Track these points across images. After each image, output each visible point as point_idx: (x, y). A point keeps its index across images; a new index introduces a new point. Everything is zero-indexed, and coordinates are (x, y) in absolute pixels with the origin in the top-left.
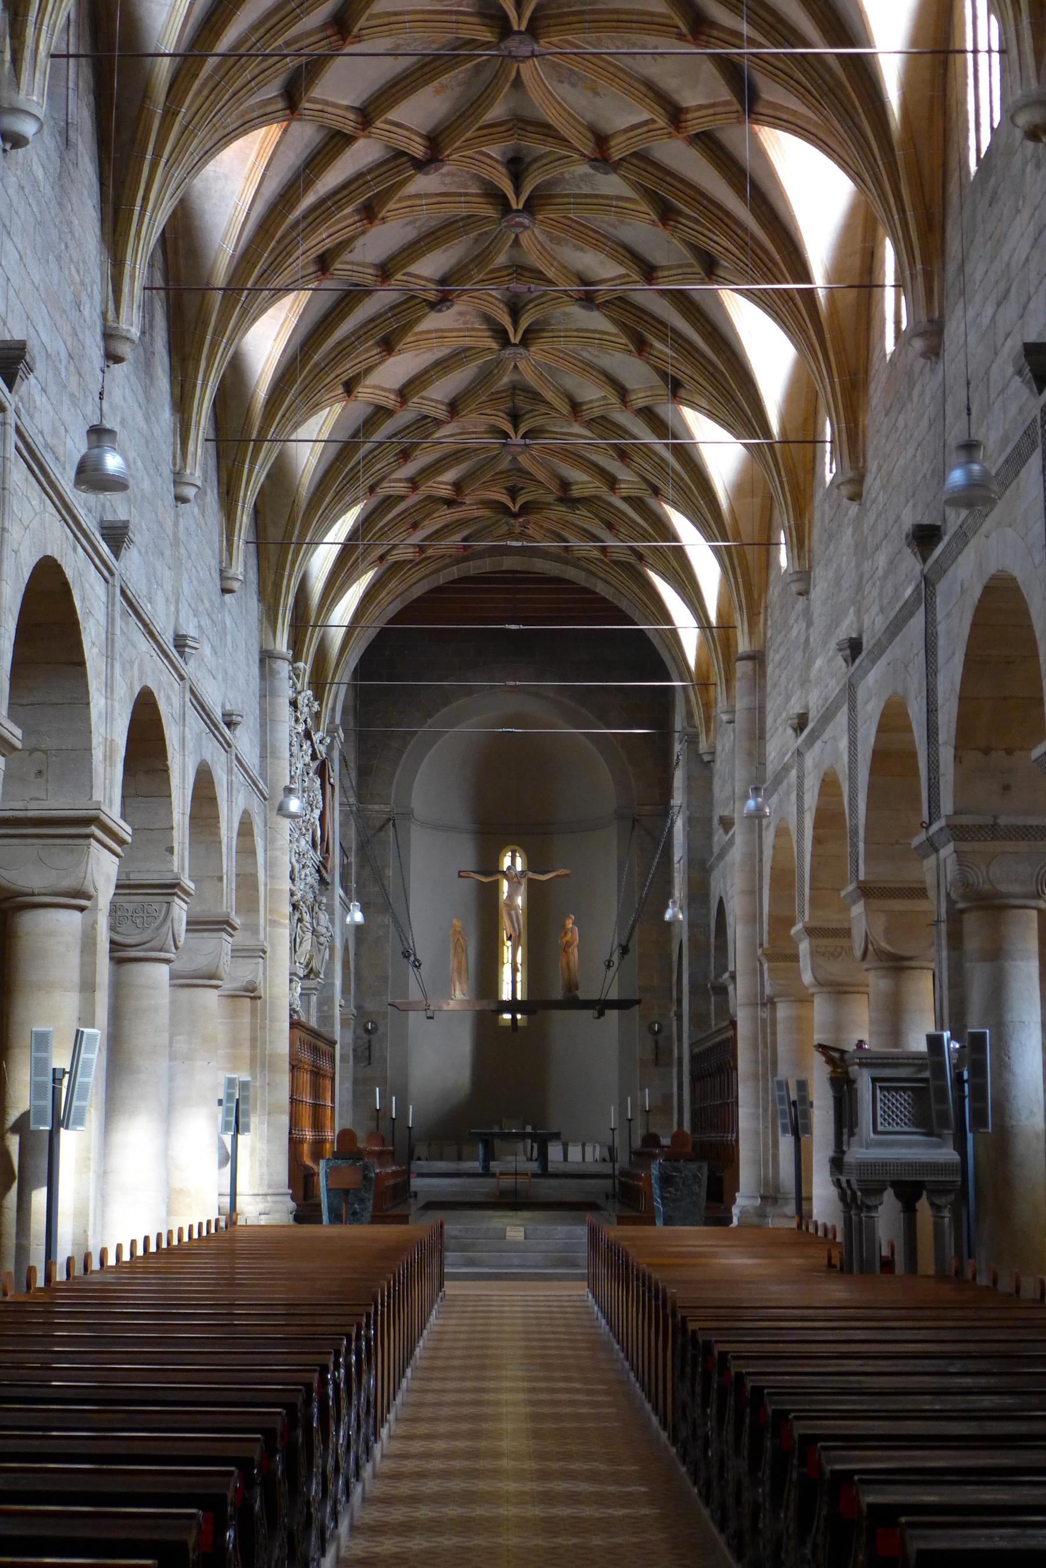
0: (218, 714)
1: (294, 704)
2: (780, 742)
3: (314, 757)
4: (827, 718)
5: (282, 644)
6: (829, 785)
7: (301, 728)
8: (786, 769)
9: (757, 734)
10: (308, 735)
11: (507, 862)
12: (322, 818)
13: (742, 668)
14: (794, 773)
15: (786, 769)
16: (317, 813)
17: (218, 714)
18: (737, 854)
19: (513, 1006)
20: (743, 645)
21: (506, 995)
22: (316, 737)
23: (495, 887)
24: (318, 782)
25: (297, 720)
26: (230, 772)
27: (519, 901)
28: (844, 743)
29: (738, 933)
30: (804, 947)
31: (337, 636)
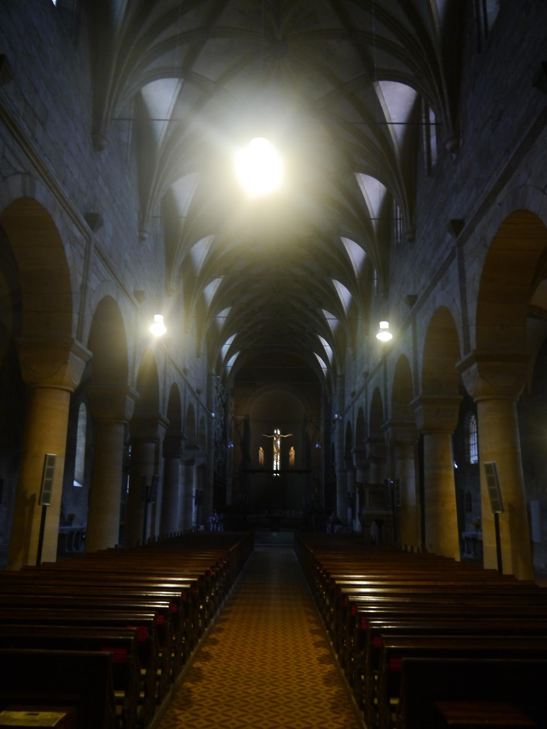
0: (195, 390)
1: (217, 387)
2: (348, 400)
3: (222, 402)
4: (360, 393)
5: (214, 371)
6: (361, 410)
7: (218, 394)
8: (349, 407)
9: (342, 397)
10: (220, 396)
11: (275, 432)
12: (224, 419)
13: (338, 379)
14: (351, 409)
15: (349, 407)
16: (223, 418)
17: (195, 390)
18: (337, 430)
19: (277, 472)
20: (339, 373)
21: (275, 469)
22: (223, 397)
23: (273, 438)
24: (223, 409)
25: (217, 392)
26: (198, 406)
27: (279, 442)
28: (364, 400)
29: (337, 452)
30: (354, 456)
31: (229, 369)
